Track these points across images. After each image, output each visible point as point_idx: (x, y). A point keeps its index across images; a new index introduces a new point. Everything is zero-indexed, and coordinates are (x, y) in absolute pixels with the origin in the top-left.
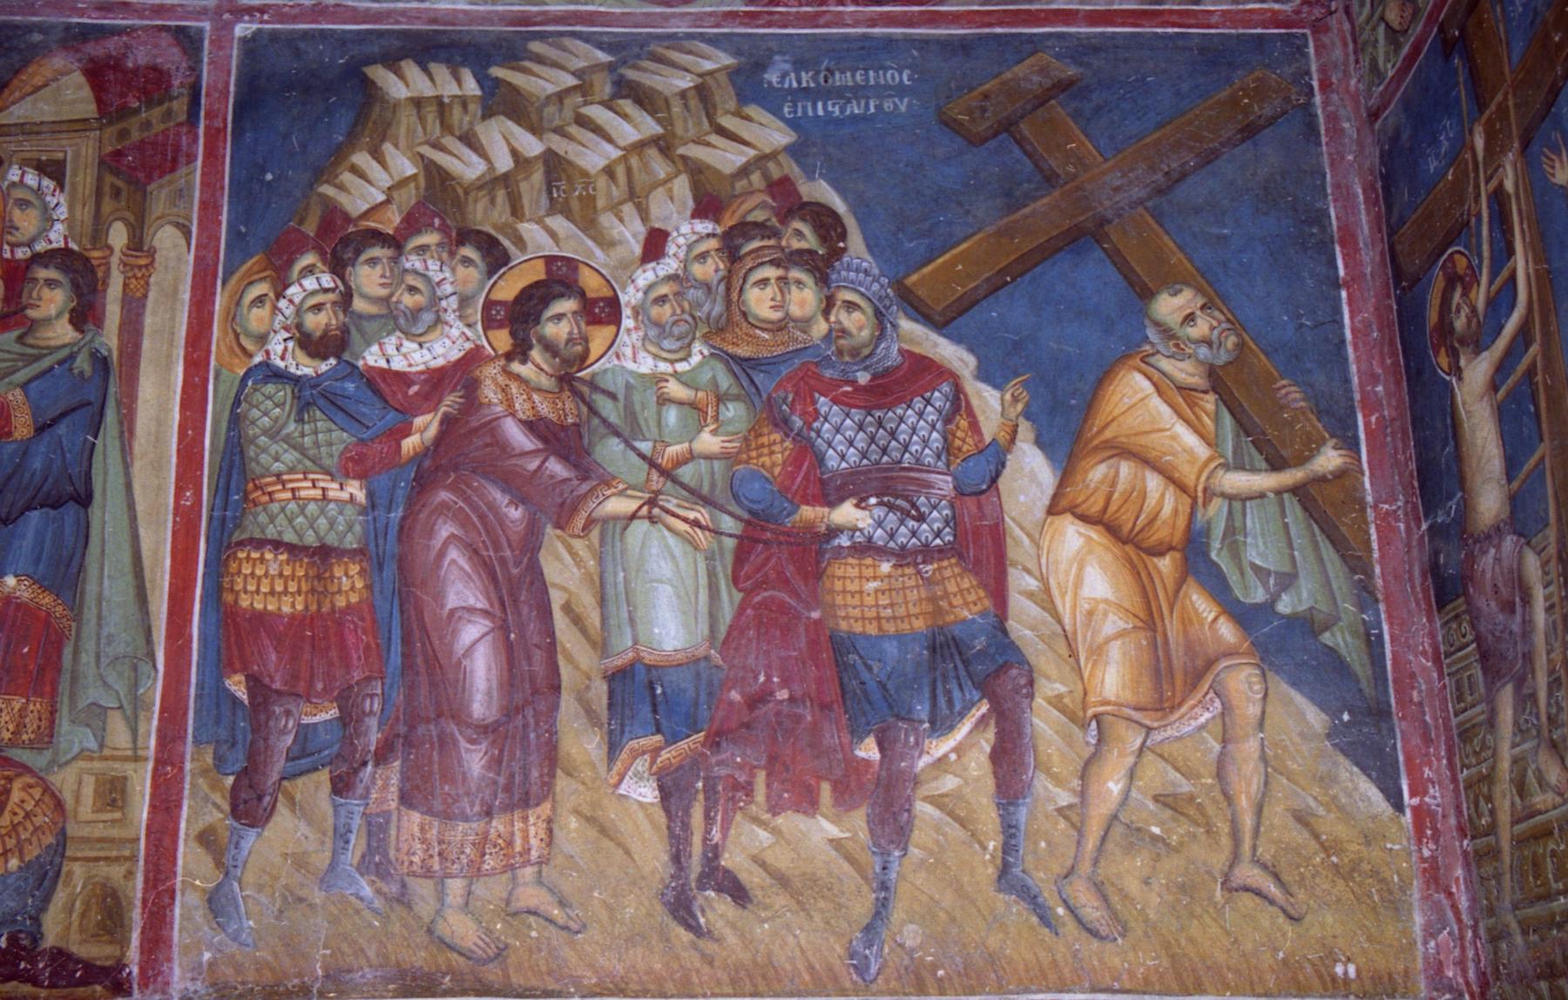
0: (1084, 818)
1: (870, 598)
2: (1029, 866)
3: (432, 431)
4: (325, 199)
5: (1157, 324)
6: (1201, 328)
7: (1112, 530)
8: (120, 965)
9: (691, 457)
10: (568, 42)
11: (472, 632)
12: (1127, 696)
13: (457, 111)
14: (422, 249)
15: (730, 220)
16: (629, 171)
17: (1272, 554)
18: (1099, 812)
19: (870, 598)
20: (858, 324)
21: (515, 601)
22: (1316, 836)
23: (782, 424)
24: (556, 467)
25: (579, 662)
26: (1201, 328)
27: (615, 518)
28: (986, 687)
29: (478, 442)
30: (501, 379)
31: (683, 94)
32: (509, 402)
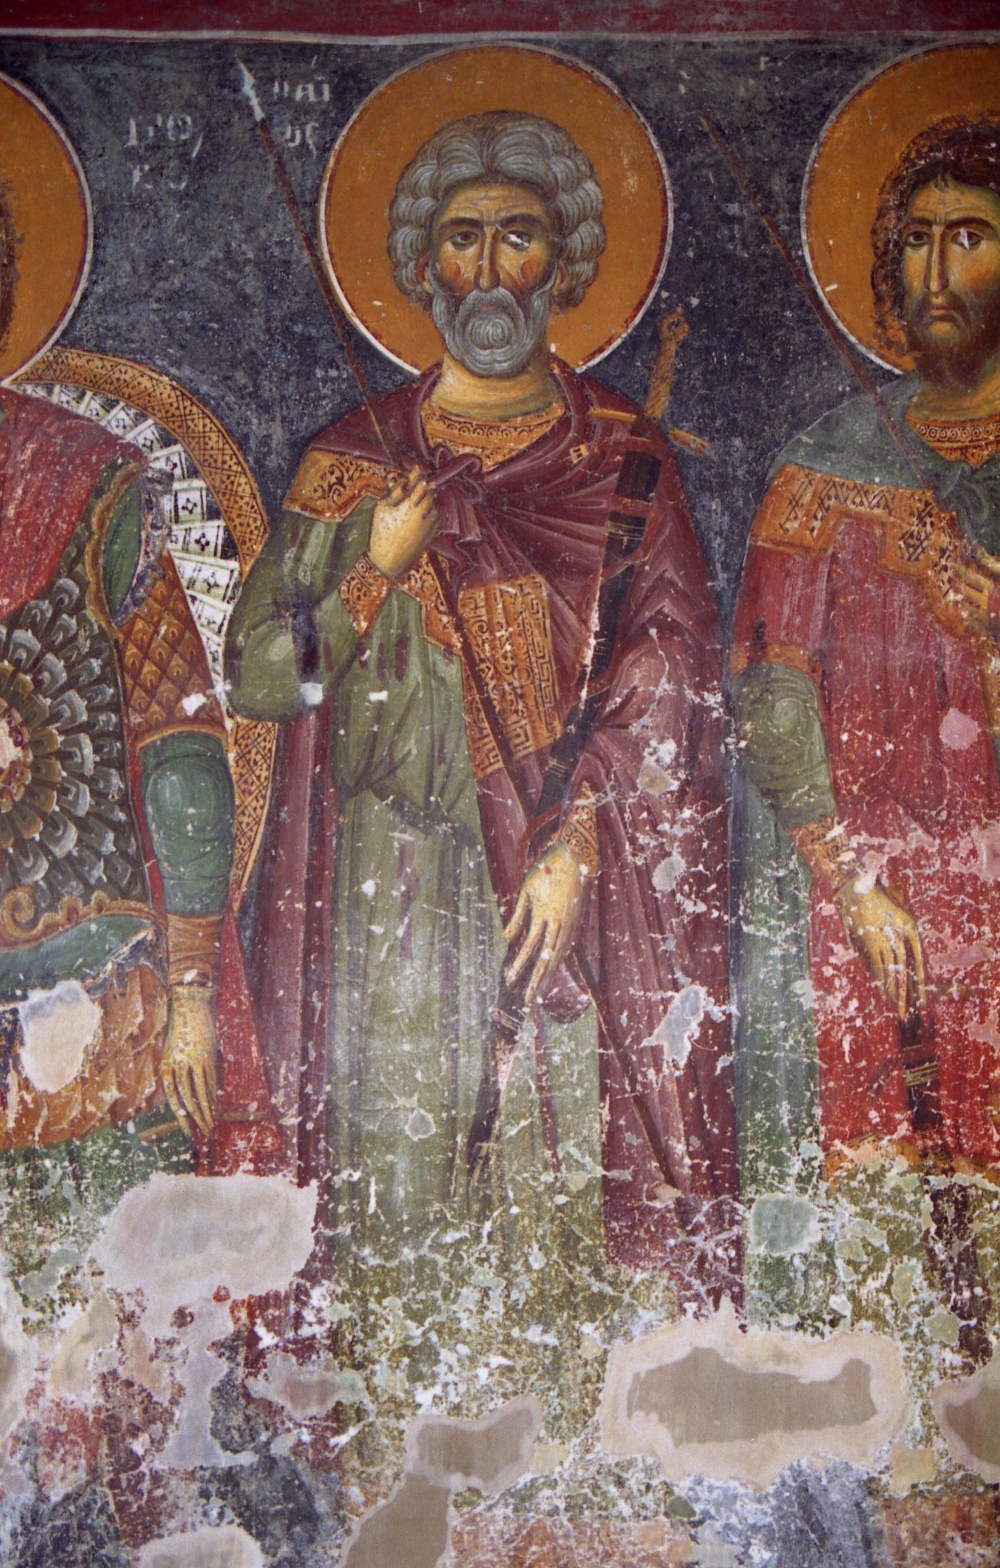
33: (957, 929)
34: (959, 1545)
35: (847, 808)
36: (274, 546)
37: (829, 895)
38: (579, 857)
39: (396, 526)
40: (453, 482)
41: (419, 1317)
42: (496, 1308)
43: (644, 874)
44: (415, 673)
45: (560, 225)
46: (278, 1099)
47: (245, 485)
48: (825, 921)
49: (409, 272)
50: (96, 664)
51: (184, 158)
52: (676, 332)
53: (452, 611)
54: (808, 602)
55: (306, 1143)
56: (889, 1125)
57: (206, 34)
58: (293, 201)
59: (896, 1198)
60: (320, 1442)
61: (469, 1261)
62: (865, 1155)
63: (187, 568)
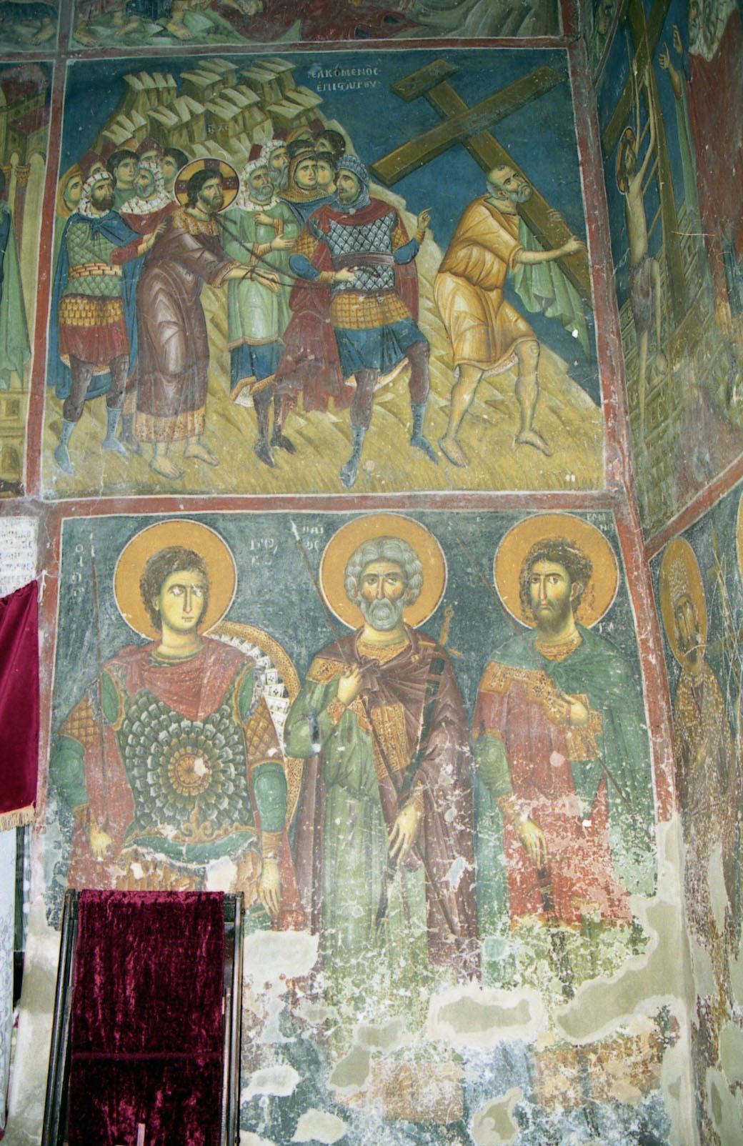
0: (452, 412)
1: (354, 313)
2: (426, 432)
3: (152, 241)
4: (105, 137)
5: (492, 184)
6: (513, 185)
7: (469, 279)
8: (19, 483)
9: (271, 250)
10: (216, 60)
11: (169, 332)
12: (474, 356)
13: (165, 95)
14: (148, 158)
15: (291, 139)
16: (244, 118)
17: (544, 289)
18: (459, 408)
19: (354, 313)
20: (350, 186)
21: (189, 319)
22: (559, 417)
23: (314, 234)
24: (208, 256)
25: (218, 345)
26: (513, 185)
27: (235, 279)
28: (407, 352)
29: (173, 245)
30: (184, 217)
31: (270, 82)
32: (187, 227)
33: (558, 834)
34: (563, 1069)
35: (516, 788)
36: (302, 694)
37: (511, 822)
38: (417, 809)
39: (348, 685)
40: (369, 668)
41: (358, 986)
42: (387, 982)
43: (441, 816)
44: (355, 740)
45: (407, 576)
46: (303, 902)
47: (292, 671)
48: (509, 832)
49: (352, 592)
50: (236, 737)
51: (271, 554)
52: (450, 614)
53: (369, 717)
54: (500, 712)
55: (314, 919)
56: (535, 909)
57: (279, 511)
58: (310, 568)
59: (538, 937)
60: (321, 1034)
61: (377, 964)
62: (526, 921)
63: (271, 701)
